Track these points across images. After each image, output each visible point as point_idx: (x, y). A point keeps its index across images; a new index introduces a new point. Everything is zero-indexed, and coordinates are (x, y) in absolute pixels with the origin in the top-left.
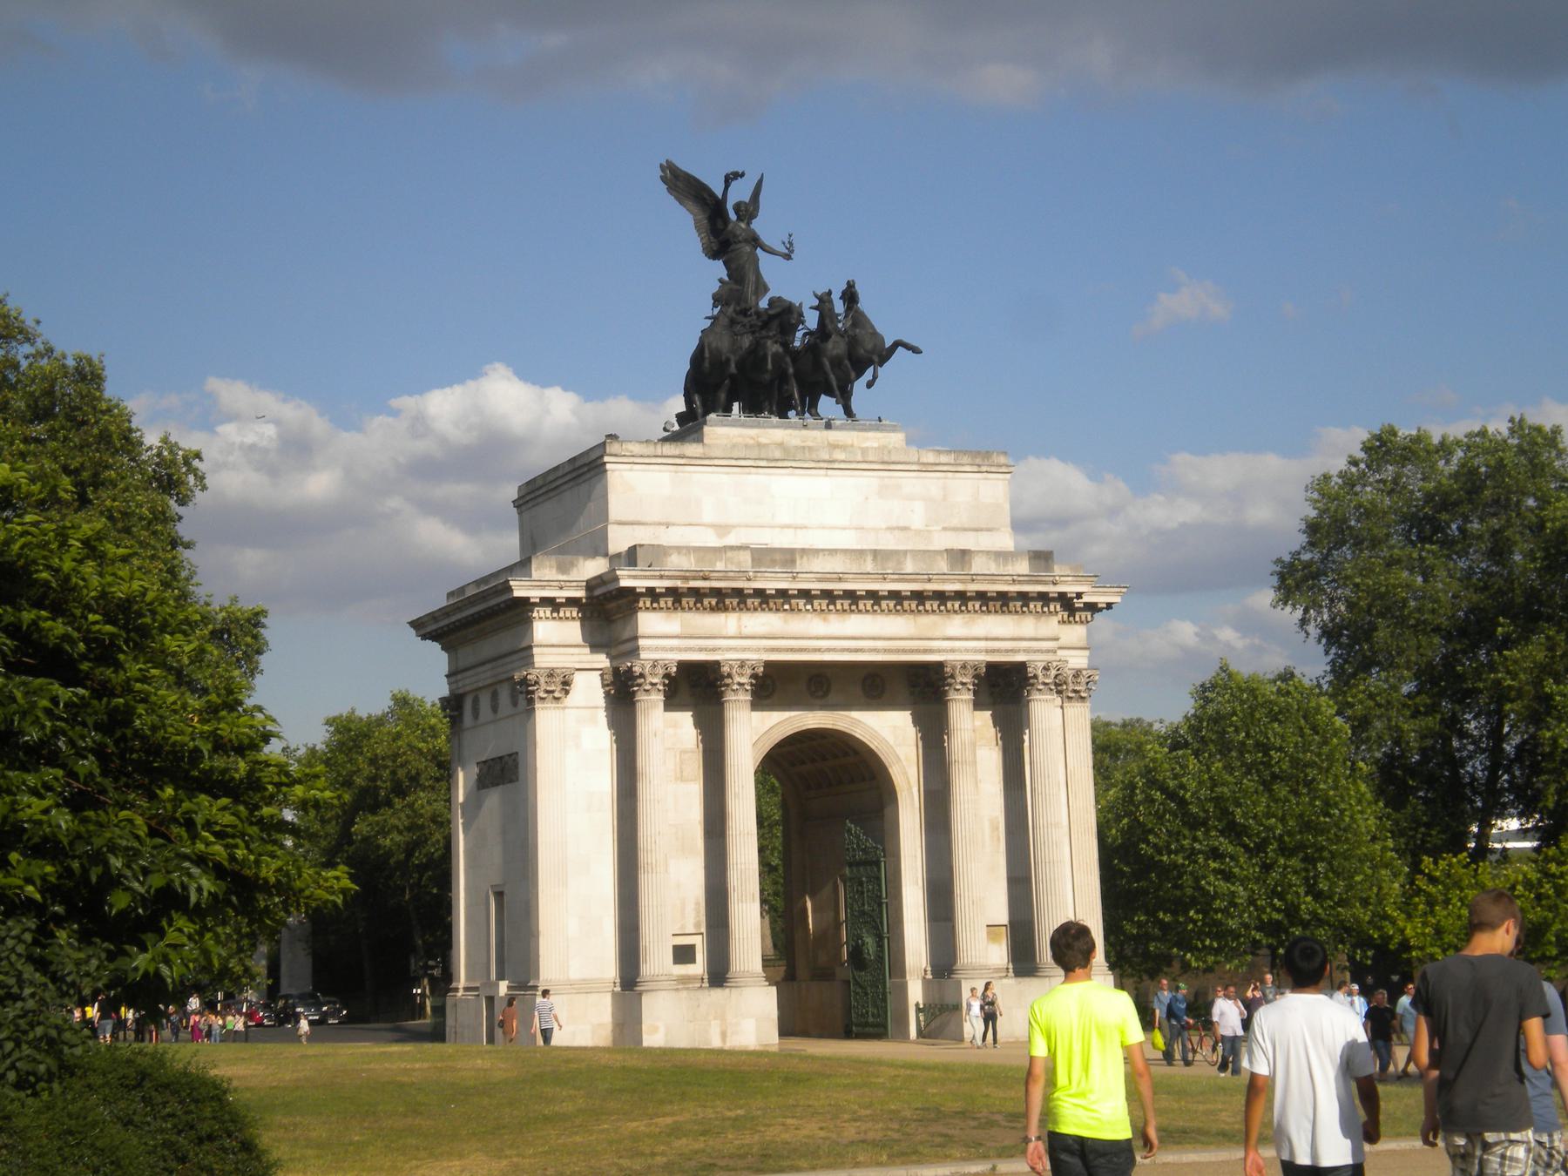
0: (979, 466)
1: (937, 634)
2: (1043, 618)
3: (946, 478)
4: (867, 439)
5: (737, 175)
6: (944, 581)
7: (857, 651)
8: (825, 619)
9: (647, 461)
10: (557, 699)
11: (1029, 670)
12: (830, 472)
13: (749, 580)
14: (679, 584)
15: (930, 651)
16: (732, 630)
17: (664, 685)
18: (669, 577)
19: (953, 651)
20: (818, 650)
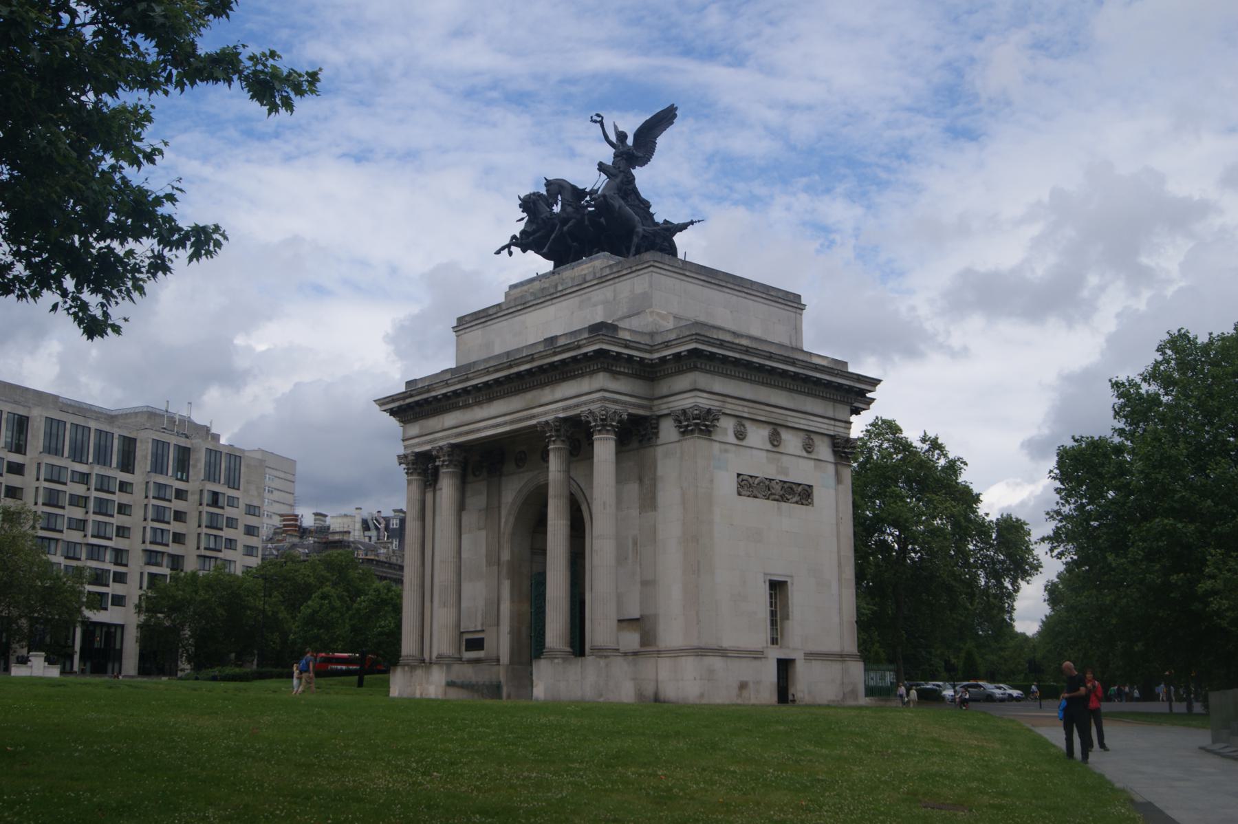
0: (631, 267)
1: (537, 404)
2: (594, 376)
3: (615, 283)
4: (583, 270)
5: (592, 117)
6: (518, 365)
7: (498, 425)
8: (481, 408)
9: (469, 325)
10: (430, 485)
11: (583, 418)
12: (554, 301)
13: (428, 391)
14: (401, 403)
15: (533, 417)
16: (439, 427)
17: (415, 469)
18: (398, 400)
19: (545, 413)
20: (479, 430)
